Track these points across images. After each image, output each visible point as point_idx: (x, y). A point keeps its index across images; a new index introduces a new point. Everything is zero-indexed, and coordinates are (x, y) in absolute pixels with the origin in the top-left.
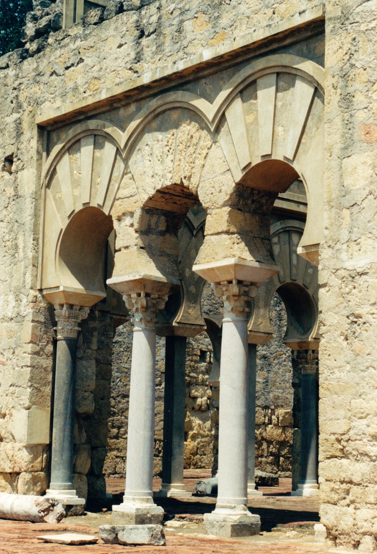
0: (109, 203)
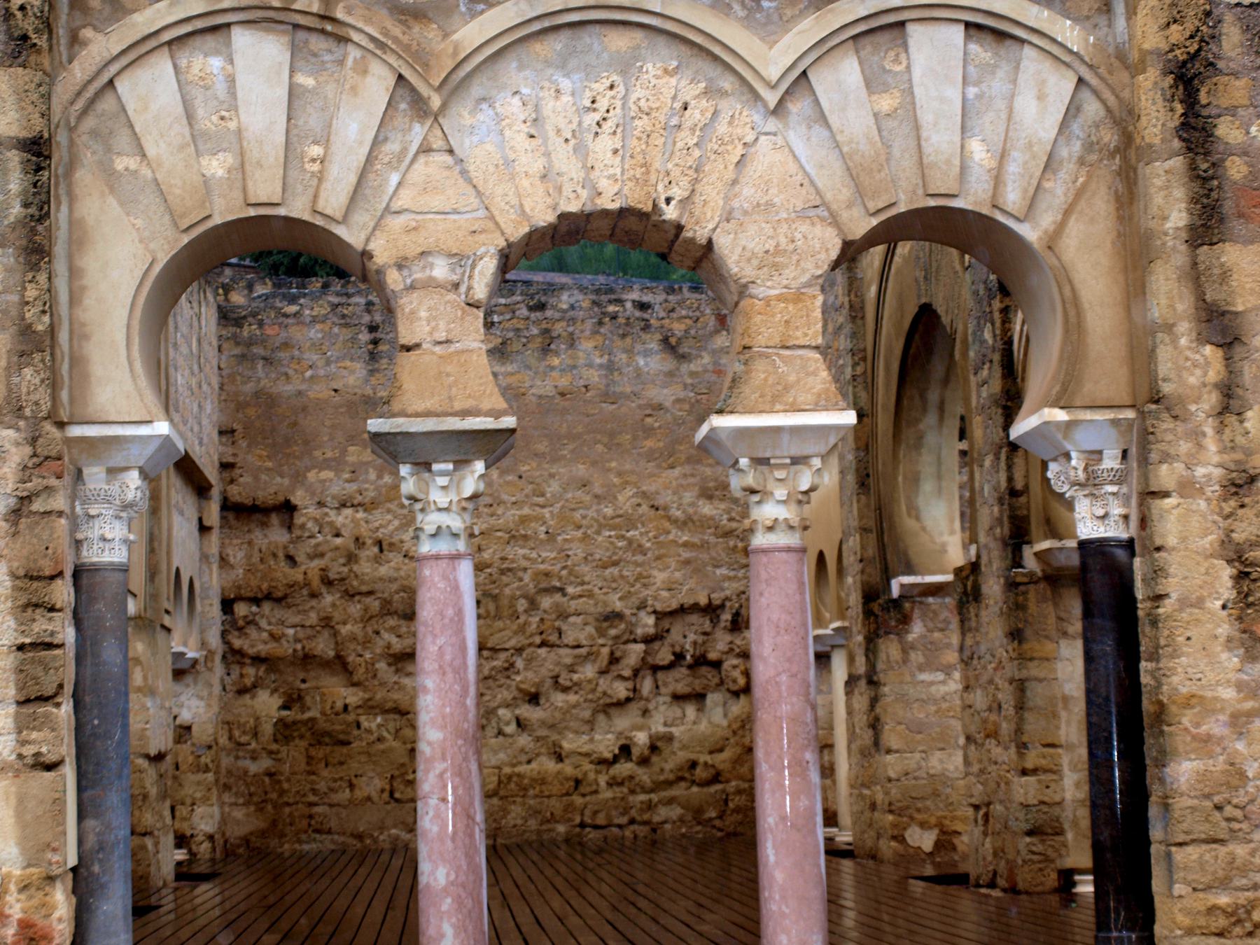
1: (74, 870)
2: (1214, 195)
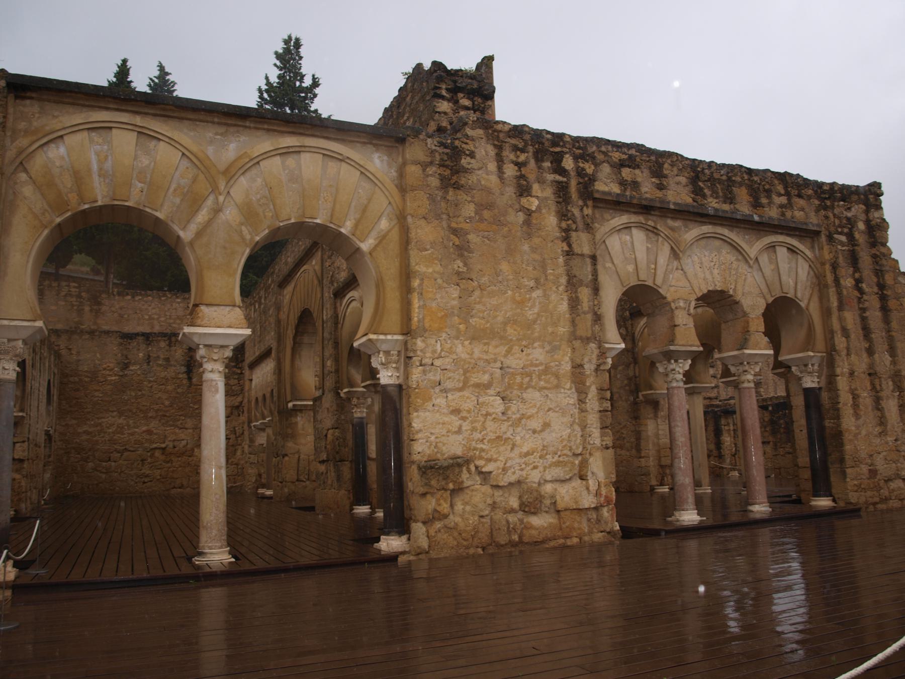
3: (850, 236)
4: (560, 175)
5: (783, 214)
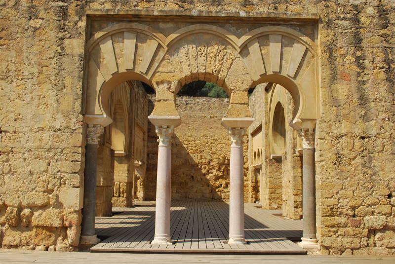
0: (151, 73)
1: (82, 209)
2: (335, 74)
3: (356, 20)
4: (62, 1)
5: (276, 8)
